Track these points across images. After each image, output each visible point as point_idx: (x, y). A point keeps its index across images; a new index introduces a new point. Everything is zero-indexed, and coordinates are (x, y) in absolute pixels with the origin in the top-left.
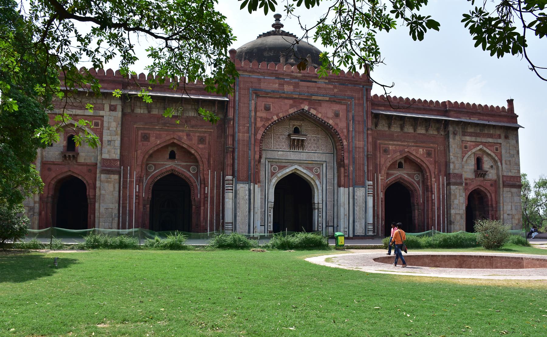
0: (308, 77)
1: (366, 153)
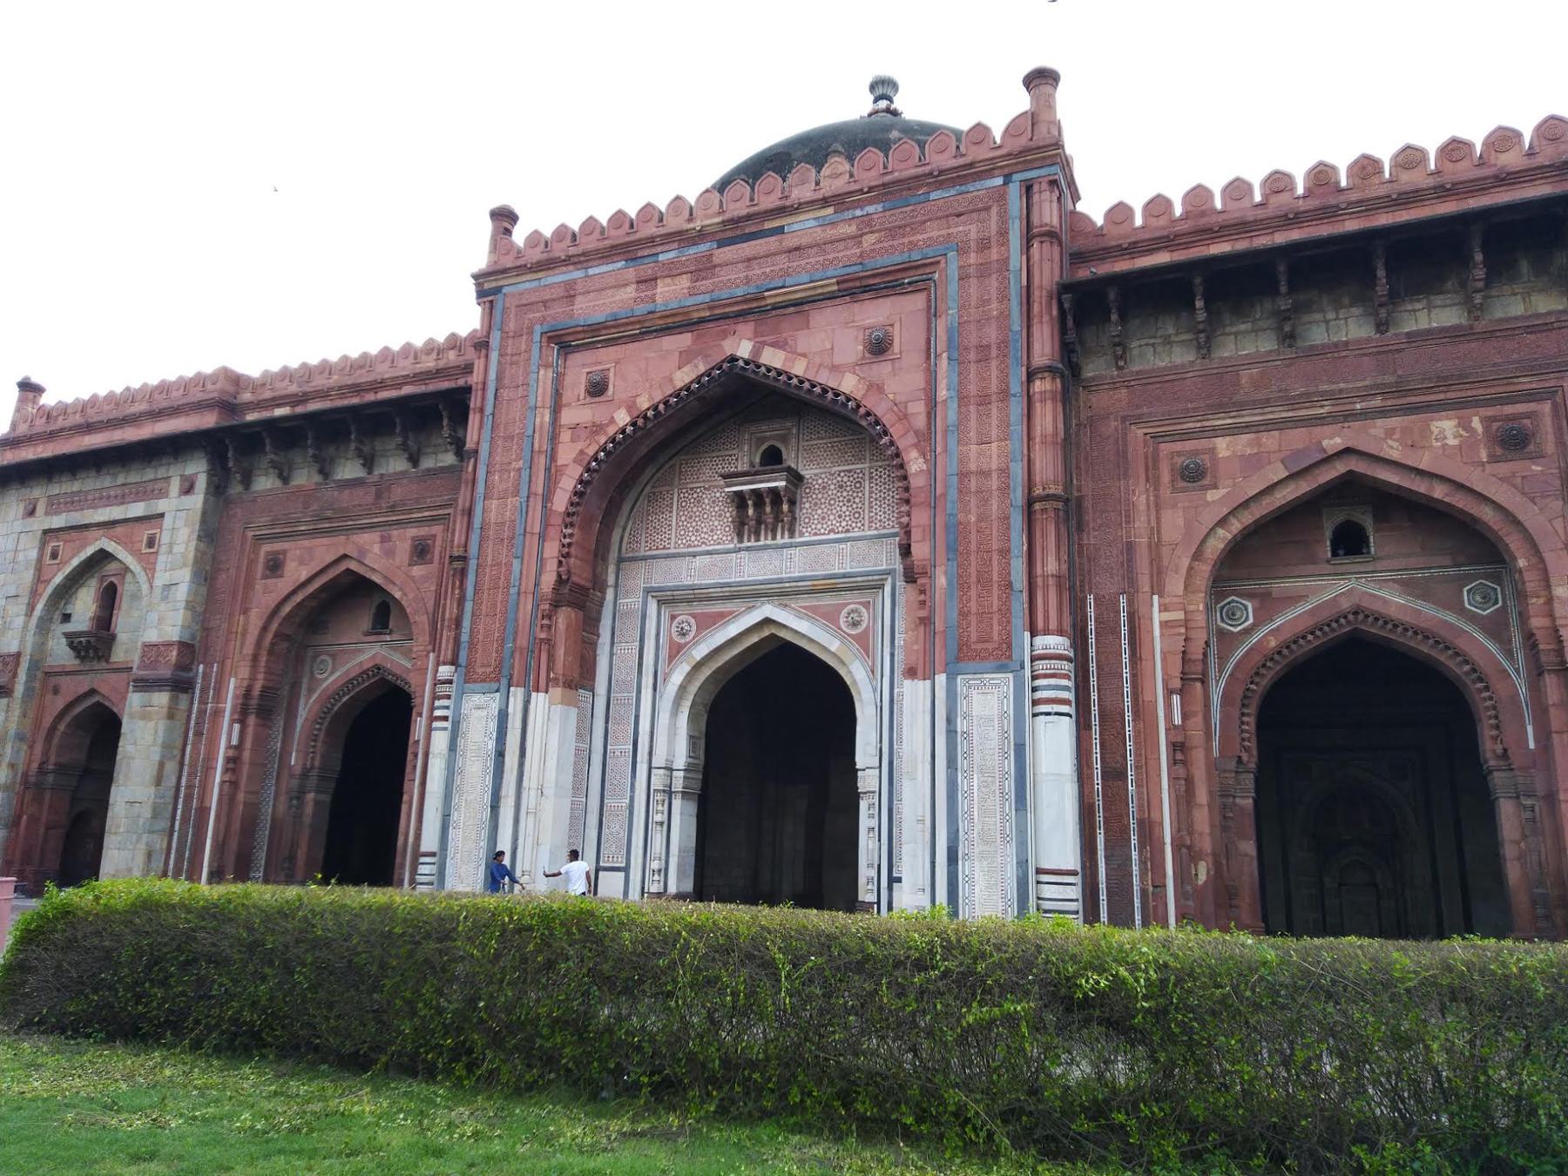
0: (749, 217)
1: (1018, 496)
